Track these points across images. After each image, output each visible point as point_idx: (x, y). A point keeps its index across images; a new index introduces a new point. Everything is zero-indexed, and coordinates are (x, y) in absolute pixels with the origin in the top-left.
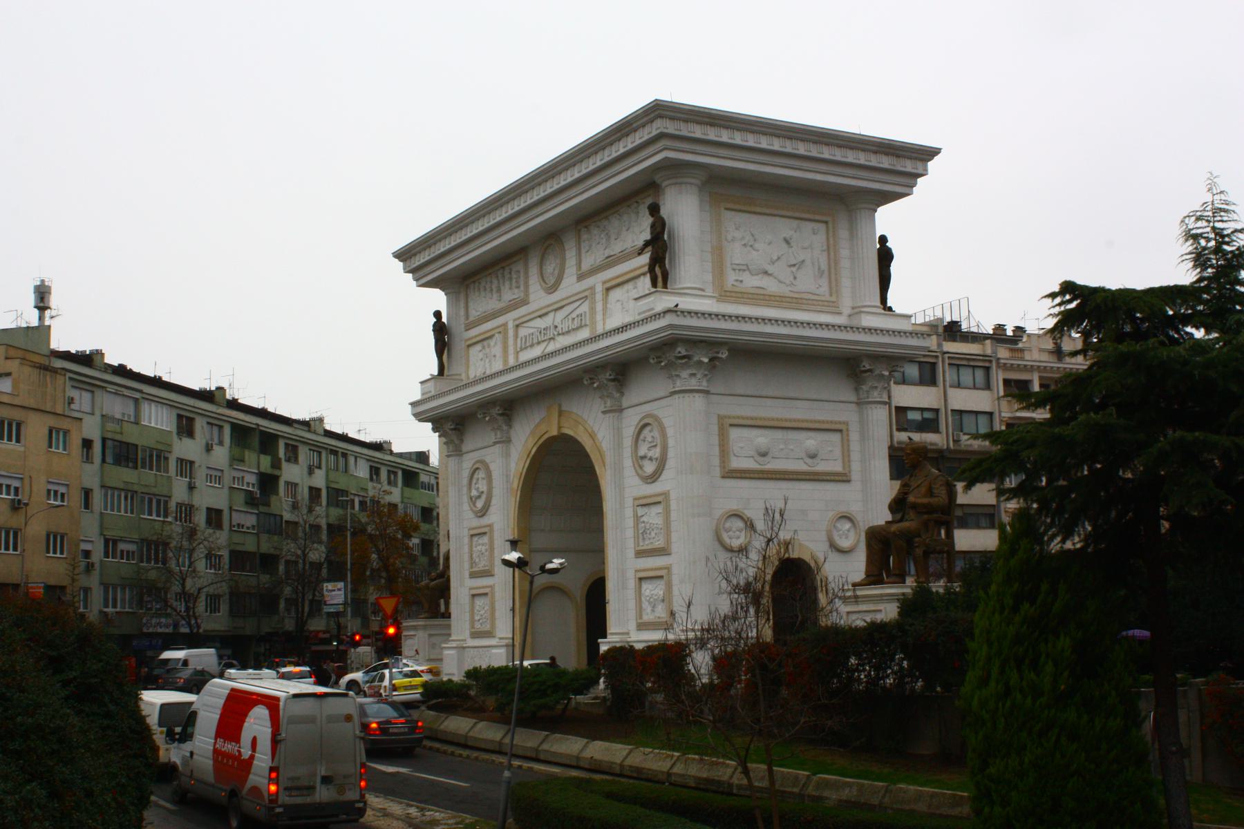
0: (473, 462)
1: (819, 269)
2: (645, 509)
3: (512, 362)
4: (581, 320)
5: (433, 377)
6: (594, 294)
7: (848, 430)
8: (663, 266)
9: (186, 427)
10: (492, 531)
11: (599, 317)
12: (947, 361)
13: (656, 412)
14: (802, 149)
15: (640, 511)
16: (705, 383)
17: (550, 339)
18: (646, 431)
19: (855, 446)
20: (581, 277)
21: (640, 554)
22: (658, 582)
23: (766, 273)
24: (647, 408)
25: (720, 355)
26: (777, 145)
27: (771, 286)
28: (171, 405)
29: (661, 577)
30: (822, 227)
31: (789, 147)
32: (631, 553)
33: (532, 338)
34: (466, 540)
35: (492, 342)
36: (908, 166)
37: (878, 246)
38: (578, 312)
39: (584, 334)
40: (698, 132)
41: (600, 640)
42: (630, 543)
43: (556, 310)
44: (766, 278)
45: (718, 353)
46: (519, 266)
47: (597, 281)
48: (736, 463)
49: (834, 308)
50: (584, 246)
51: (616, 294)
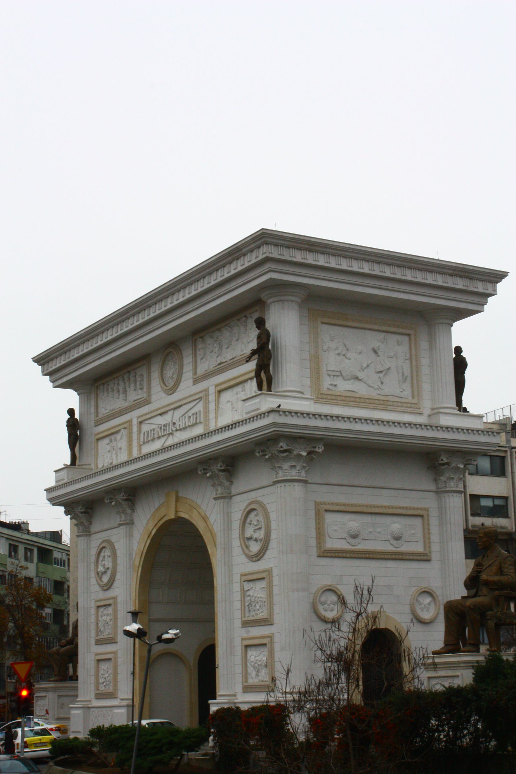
0: (100, 541)
1: (403, 375)
2: (251, 584)
3: (135, 454)
4: (196, 418)
5: (66, 467)
6: (207, 395)
7: (428, 515)
8: (267, 372)
10: (116, 603)
11: (212, 415)
13: (260, 499)
14: (388, 272)
15: (247, 586)
16: (303, 474)
17: (169, 434)
18: (252, 516)
19: (434, 530)
20: (196, 381)
21: (246, 624)
22: (262, 649)
23: (357, 378)
24: (253, 495)
25: (317, 450)
26: (366, 268)
27: (361, 389)
29: (265, 645)
30: (405, 339)
31: (377, 270)
32: (238, 623)
33: (154, 433)
34: (93, 611)
35: (118, 436)
36: (480, 287)
37: (454, 356)
38: (193, 411)
39: (199, 430)
40: (298, 256)
41: (210, 701)
42: (238, 615)
43: (174, 409)
44: (357, 383)
45: (315, 447)
46: (143, 371)
48: (331, 544)
50: (200, 354)
51: (226, 396)
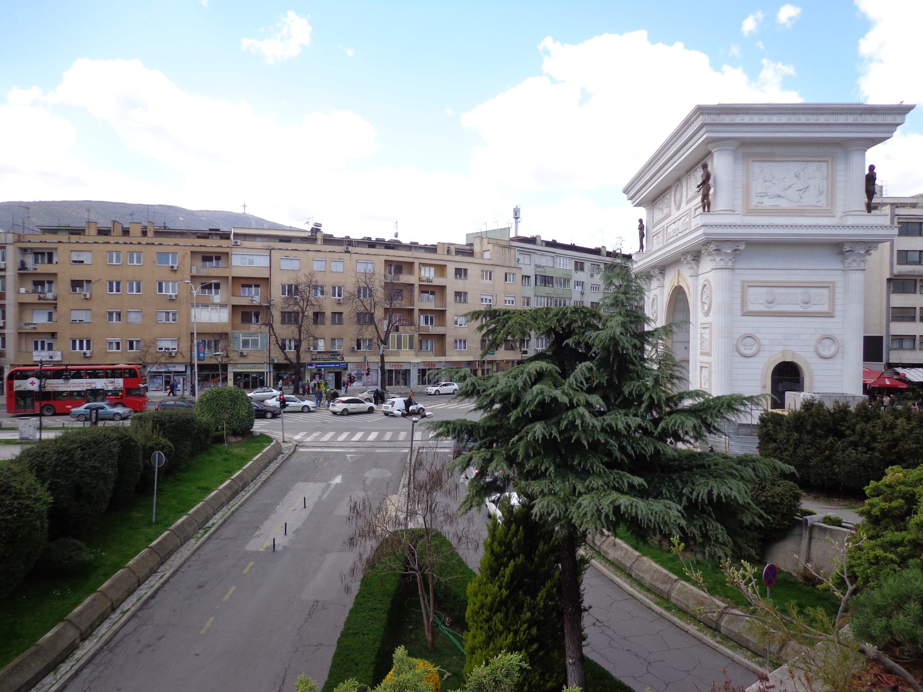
1: (819, 190)
7: (834, 286)
9: (579, 266)
14: (803, 119)
16: (730, 264)
19: (839, 296)
21: (702, 354)
25: (740, 248)
27: (783, 204)
28: (571, 257)
30: (824, 164)
31: (793, 119)
36: (889, 119)
37: (867, 172)
40: (727, 119)
45: (738, 246)
48: (751, 308)
49: (829, 213)
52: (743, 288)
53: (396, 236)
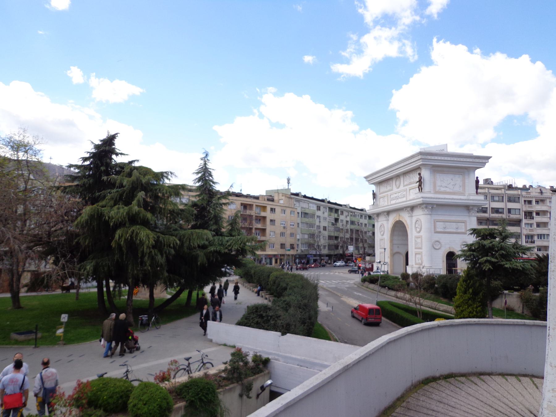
2: (417, 239)
5: (372, 205)
6: (407, 190)
8: (421, 187)
9: (319, 208)
11: (408, 195)
12: (507, 196)
14: (455, 159)
15: (416, 239)
18: (417, 222)
20: (404, 186)
21: (416, 248)
22: (419, 255)
23: (446, 187)
24: (418, 217)
26: (449, 159)
27: (448, 190)
28: (316, 204)
29: (420, 254)
30: (461, 176)
31: (452, 159)
32: (414, 248)
34: (379, 240)
35: (385, 198)
36: (484, 161)
37: (476, 179)
39: (404, 199)
40: (429, 157)
42: (414, 246)
44: (446, 188)
46: (391, 182)
47: (408, 187)
48: (438, 230)
49: (463, 194)
50: (405, 179)
51: (411, 191)
52: (434, 222)
53: (241, 191)
